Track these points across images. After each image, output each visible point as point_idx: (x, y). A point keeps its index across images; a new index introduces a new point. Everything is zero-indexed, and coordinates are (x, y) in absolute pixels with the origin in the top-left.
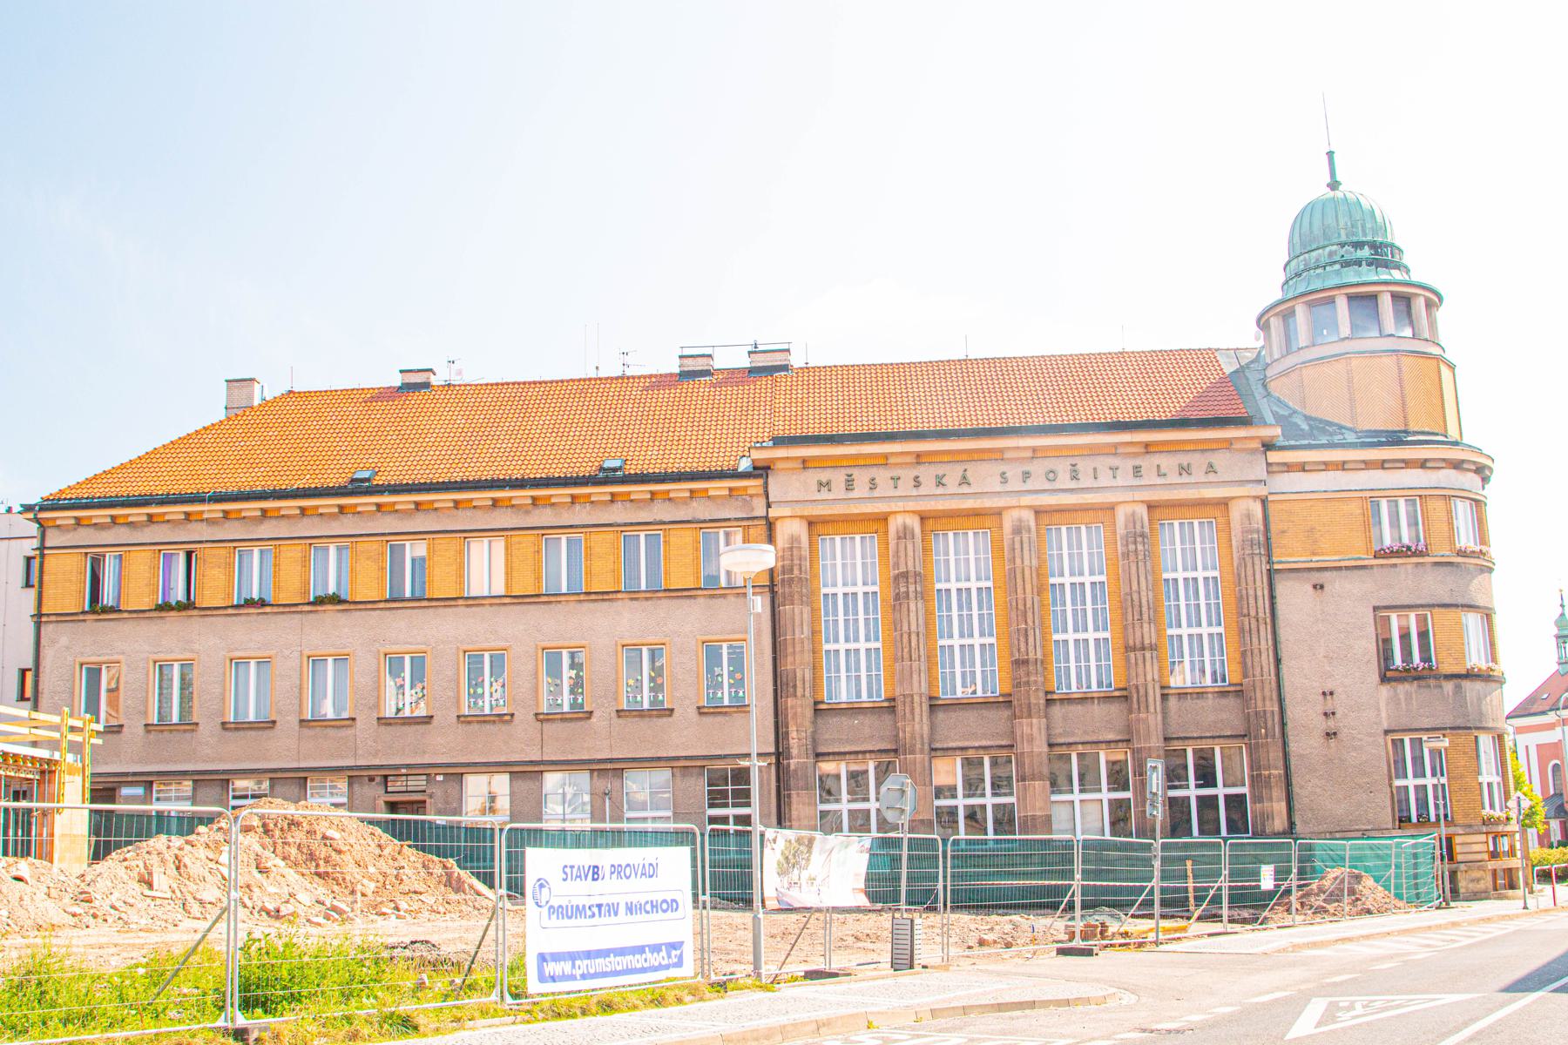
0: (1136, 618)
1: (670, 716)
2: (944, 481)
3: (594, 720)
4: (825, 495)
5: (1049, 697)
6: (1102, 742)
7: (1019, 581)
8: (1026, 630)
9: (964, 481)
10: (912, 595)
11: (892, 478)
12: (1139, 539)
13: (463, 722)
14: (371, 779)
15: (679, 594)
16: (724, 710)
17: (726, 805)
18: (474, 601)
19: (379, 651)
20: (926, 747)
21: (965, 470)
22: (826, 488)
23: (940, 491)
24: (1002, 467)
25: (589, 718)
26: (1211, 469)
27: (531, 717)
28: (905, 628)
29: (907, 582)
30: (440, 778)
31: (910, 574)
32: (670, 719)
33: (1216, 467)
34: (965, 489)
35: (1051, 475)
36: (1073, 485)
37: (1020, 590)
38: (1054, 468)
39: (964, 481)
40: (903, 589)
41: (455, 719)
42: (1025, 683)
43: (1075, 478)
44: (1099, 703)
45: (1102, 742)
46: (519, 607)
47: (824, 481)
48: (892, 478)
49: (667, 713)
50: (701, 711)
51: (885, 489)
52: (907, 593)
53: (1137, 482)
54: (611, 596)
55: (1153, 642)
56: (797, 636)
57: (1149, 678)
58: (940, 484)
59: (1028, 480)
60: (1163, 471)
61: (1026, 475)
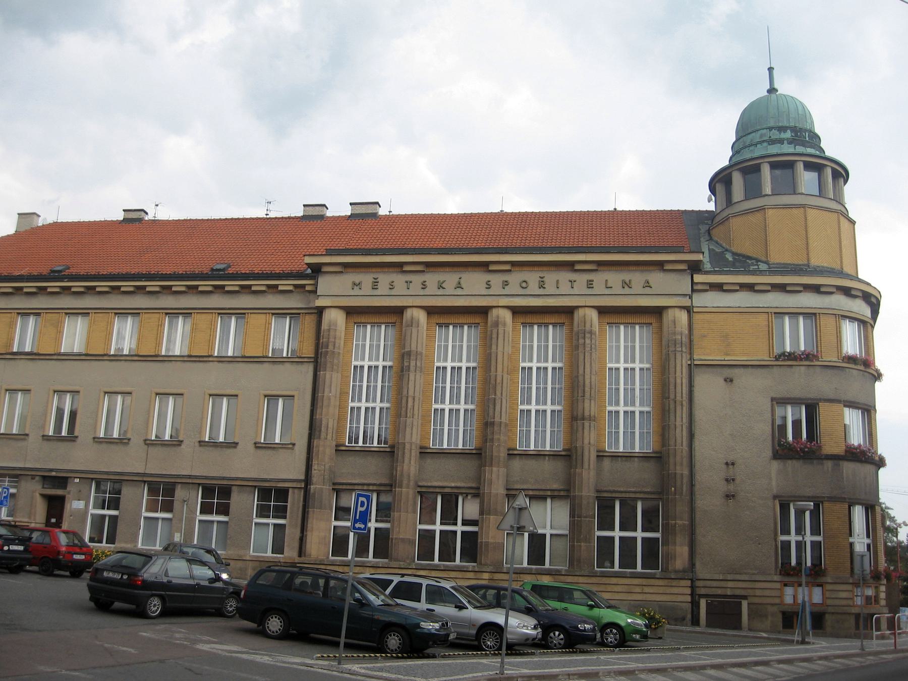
0: (580, 395)
1: (235, 447)
2: (443, 285)
3: (183, 446)
4: (357, 291)
5: (511, 452)
6: (548, 490)
7: (493, 362)
8: (495, 399)
9: (459, 286)
10: (412, 368)
11: (407, 282)
12: (588, 335)
13: (97, 442)
14: (33, 477)
15: (252, 360)
16: (275, 446)
17: (268, 517)
18: (169, 359)
19: (151, 391)
20: (412, 483)
21: (460, 279)
22: (358, 287)
23: (441, 292)
24: (489, 277)
25: (180, 445)
26: (647, 285)
27: (142, 443)
28: (405, 393)
29: (410, 359)
30: (77, 480)
31: (412, 354)
32: (235, 450)
33: (651, 284)
34: (459, 291)
35: (524, 284)
36: (541, 292)
37: (493, 369)
38: (526, 279)
39: (459, 286)
40: (406, 364)
41: (92, 441)
42: (490, 440)
43: (541, 286)
44: (549, 460)
45: (548, 490)
46: (144, 364)
47: (357, 282)
48: (407, 282)
49: (233, 445)
50: (257, 446)
51: (400, 288)
52: (409, 367)
53: (590, 292)
54: (205, 359)
55: (592, 414)
56: (326, 394)
57: (586, 441)
58: (440, 287)
59: (506, 287)
60: (609, 285)
61: (506, 284)
